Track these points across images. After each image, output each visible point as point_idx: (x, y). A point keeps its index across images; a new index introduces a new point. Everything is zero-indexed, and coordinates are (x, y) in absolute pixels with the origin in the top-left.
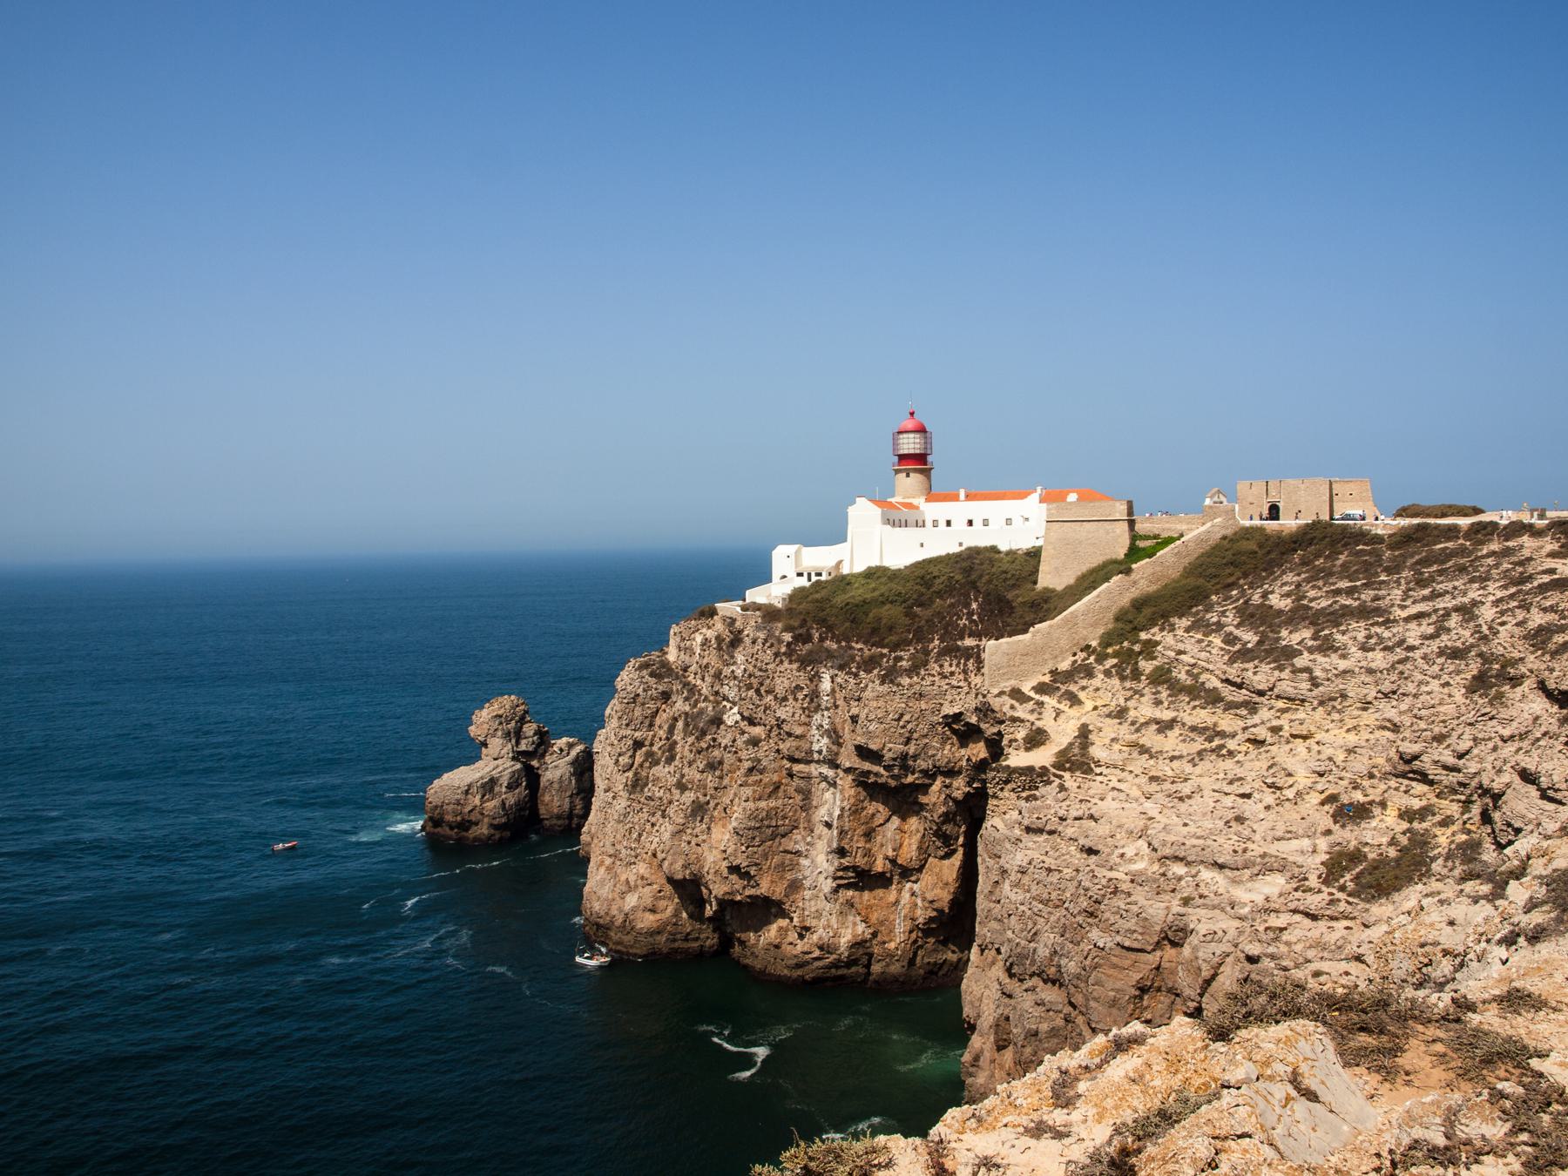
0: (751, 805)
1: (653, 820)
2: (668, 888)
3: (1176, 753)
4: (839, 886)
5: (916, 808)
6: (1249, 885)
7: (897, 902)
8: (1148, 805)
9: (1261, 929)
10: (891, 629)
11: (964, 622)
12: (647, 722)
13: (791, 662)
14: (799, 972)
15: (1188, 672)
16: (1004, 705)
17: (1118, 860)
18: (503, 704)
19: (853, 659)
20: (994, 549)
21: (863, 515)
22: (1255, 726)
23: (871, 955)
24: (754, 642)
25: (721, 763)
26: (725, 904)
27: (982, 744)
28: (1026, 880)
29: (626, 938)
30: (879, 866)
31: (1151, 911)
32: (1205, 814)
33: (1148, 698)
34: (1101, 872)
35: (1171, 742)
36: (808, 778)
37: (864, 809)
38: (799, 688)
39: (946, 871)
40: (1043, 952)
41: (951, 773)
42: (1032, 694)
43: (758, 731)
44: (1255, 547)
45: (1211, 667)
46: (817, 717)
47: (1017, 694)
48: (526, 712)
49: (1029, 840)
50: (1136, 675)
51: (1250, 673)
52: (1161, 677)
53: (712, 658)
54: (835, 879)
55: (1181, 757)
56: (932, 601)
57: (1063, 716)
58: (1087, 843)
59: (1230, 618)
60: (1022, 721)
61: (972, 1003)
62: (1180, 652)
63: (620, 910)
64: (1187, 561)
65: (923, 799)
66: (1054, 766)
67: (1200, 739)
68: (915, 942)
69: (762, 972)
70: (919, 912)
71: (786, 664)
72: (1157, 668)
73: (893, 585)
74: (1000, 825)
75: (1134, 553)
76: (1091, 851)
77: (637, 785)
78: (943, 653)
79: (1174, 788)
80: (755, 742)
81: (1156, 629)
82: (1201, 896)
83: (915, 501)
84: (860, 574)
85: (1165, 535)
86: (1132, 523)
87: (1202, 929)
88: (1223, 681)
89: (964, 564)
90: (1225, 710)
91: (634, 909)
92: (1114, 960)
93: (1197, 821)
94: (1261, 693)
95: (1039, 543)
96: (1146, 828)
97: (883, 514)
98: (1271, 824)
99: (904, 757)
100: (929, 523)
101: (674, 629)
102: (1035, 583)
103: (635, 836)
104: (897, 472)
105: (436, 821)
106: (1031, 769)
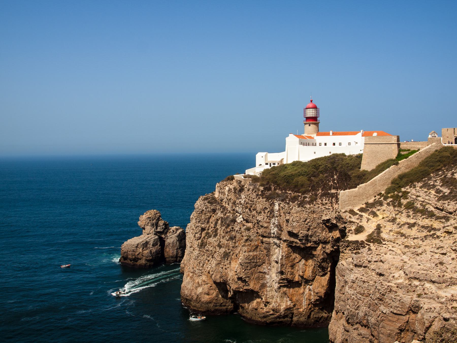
0: (246, 254)
1: (209, 259)
2: (214, 286)
3: (416, 236)
4: (281, 286)
5: (312, 256)
6: (445, 290)
7: (303, 293)
8: (404, 257)
9: (450, 307)
10: (302, 186)
11: (331, 183)
12: (207, 221)
13: (263, 198)
14: (265, 320)
15: (421, 204)
16: (346, 216)
17: (392, 278)
18: (151, 213)
19: (287, 197)
20: (343, 155)
21: (292, 141)
22: (448, 226)
23: (293, 314)
24: (248, 190)
25: (235, 237)
26: (236, 292)
27: (338, 232)
28: (355, 285)
29: (197, 305)
30: (297, 279)
31: (405, 299)
32: (427, 261)
33: (404, 214)
34: (385, 283)
35: (414, 232)
36: (269, 243)
37: (291, 256)
38: (266, 208)
39: (323, 281)
40: (361, 314)
41: (325, 243)
42: (358, 212)
43: (249, 225)
44: (449, 155)
45: (430, 202)
46: (273, 220)
47: (352, 212)
48: (160, 216)
49: (356, 270)
50: (400, 205)
51: (446, 205)
52: (410, 206)
53: (232, 196)
54: (279, 283)
55: (417, 238)
56: (319, 175)
57: (370, 221)
58: (380, 271)
59: (438, 183)
60: (354, 223)
61: (332, 333)
62: (418, 196)
63: (195, 294)
64: (421, 160)
65: (314, 253)
66: (366, 241)
67: (426, 231)
68: (310, 309)
69: (250, 319)
70: (312, 297)
71: (261, 199)
72: (408, 203)
73: (303, 168)
74: (345, 264)
75: (400, 157)
76: (381, 275)
77: (202, 245)
78: (323, 195)
79: (415, 250)
80: (248, 229)
81: (408, 187)
82: (425, 294)
83: (312, 136)
84: (290, 164)
85: (412, 149)
86: (399, 145)
87: (426, 307)
88: (435, 208)
89: (332, 161)
90: (436, 220)
91: (201, 293)
92: (390, 318)
93: (424, 264)
94: (451, 213)
95: (362, 152)
96: (403, 266)
97: (300, 141)
98: (454, 266)
99: (307, 236)
100: (318, 144)
101: (218, 185)
102: (360, 168)
103: (201, 265)
104: (305, 124)
105: (125, 258)
106: (357, 242)
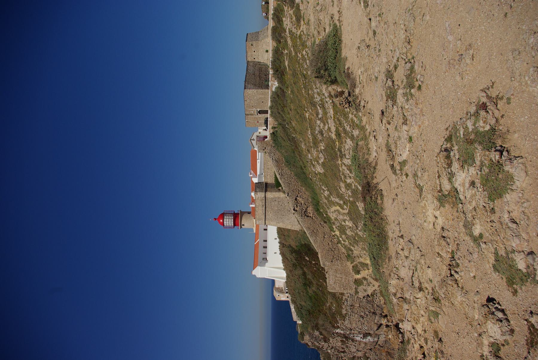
104: (241, 227)
